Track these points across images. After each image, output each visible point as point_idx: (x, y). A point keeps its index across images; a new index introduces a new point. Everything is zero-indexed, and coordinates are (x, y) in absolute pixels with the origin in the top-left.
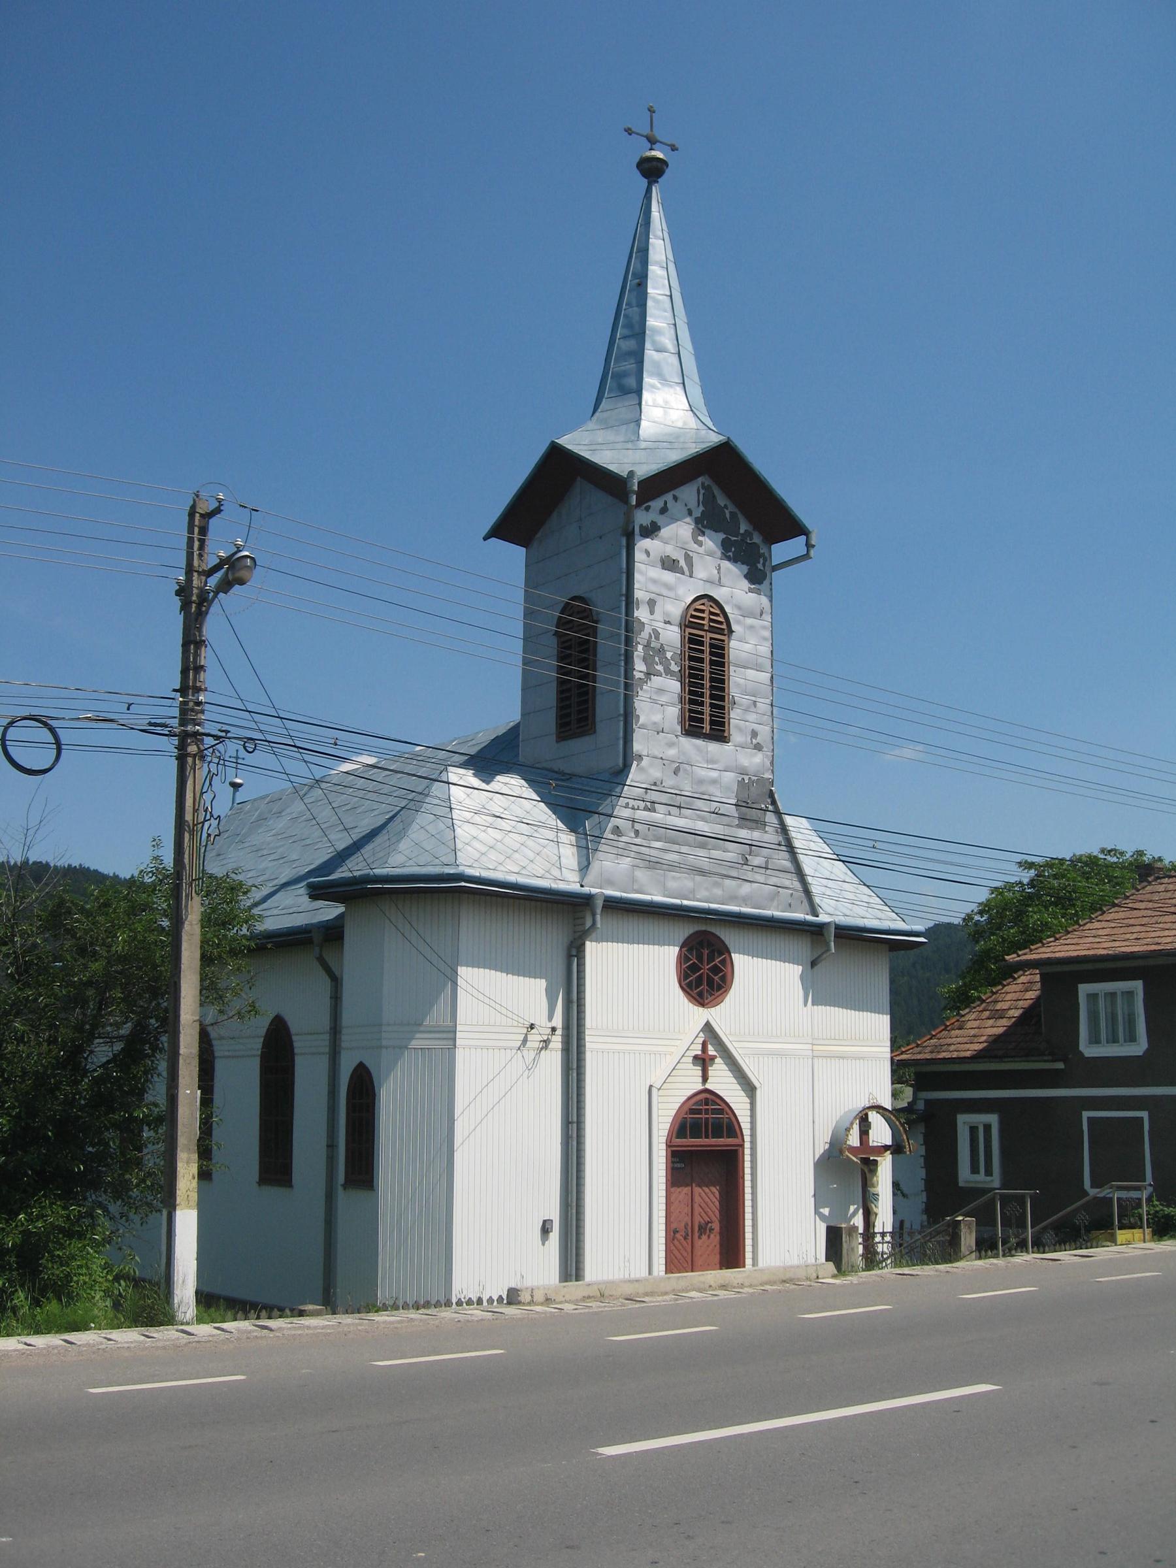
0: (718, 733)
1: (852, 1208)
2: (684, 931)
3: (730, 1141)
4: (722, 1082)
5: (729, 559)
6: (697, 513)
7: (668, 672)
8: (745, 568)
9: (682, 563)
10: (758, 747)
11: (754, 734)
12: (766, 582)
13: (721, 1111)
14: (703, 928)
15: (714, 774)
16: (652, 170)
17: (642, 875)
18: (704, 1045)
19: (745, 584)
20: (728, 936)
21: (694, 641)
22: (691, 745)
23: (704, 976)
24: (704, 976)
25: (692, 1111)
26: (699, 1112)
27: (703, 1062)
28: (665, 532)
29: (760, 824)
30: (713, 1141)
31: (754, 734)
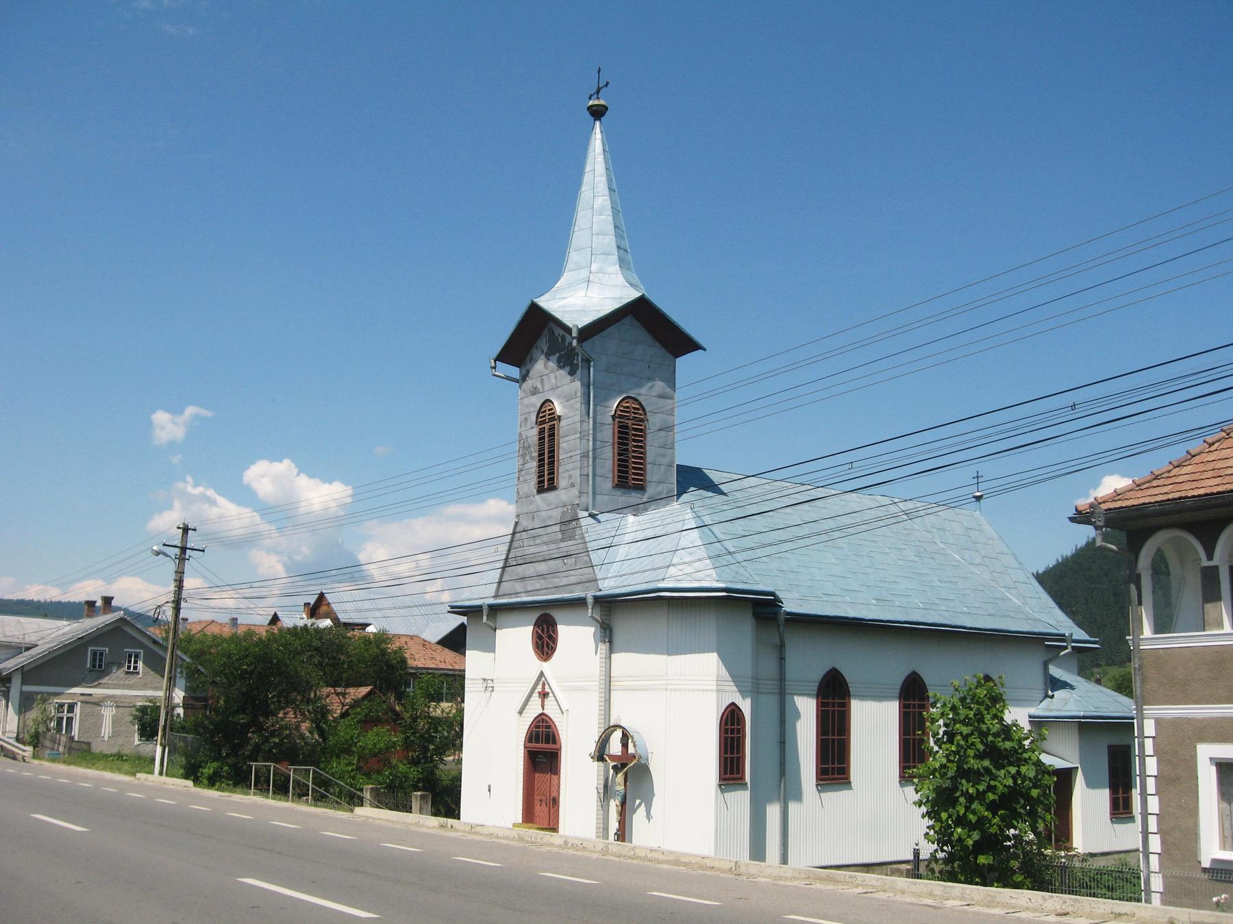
0: (552, 487)
1: (638, 802)
2: (534, 616)
3: (550, 746)
4: (551, 710)
5: (561, 368)
6: (545, 350)
7: (532, 458)
8: (568, 368)
9: (539, 386)
10: (573, 485)
11: (570, 477)
12: (579, 372)
13: (549, 727)
14: (543, 612)
15: (550, 512)
16: (598, 113)
17: (519, 587)
18: (544, 685)
19: (569, 377)
20: (557, 615)
21: (541, 431)
22: (538, 498)
23: (545, 645)
24: (545, 645)
25: (538, 727)
26: (538, 727)
27: (544, 695)
28: (531, 373)
29: (572, 538)
30: (544, 745)
31: (570, 477)
